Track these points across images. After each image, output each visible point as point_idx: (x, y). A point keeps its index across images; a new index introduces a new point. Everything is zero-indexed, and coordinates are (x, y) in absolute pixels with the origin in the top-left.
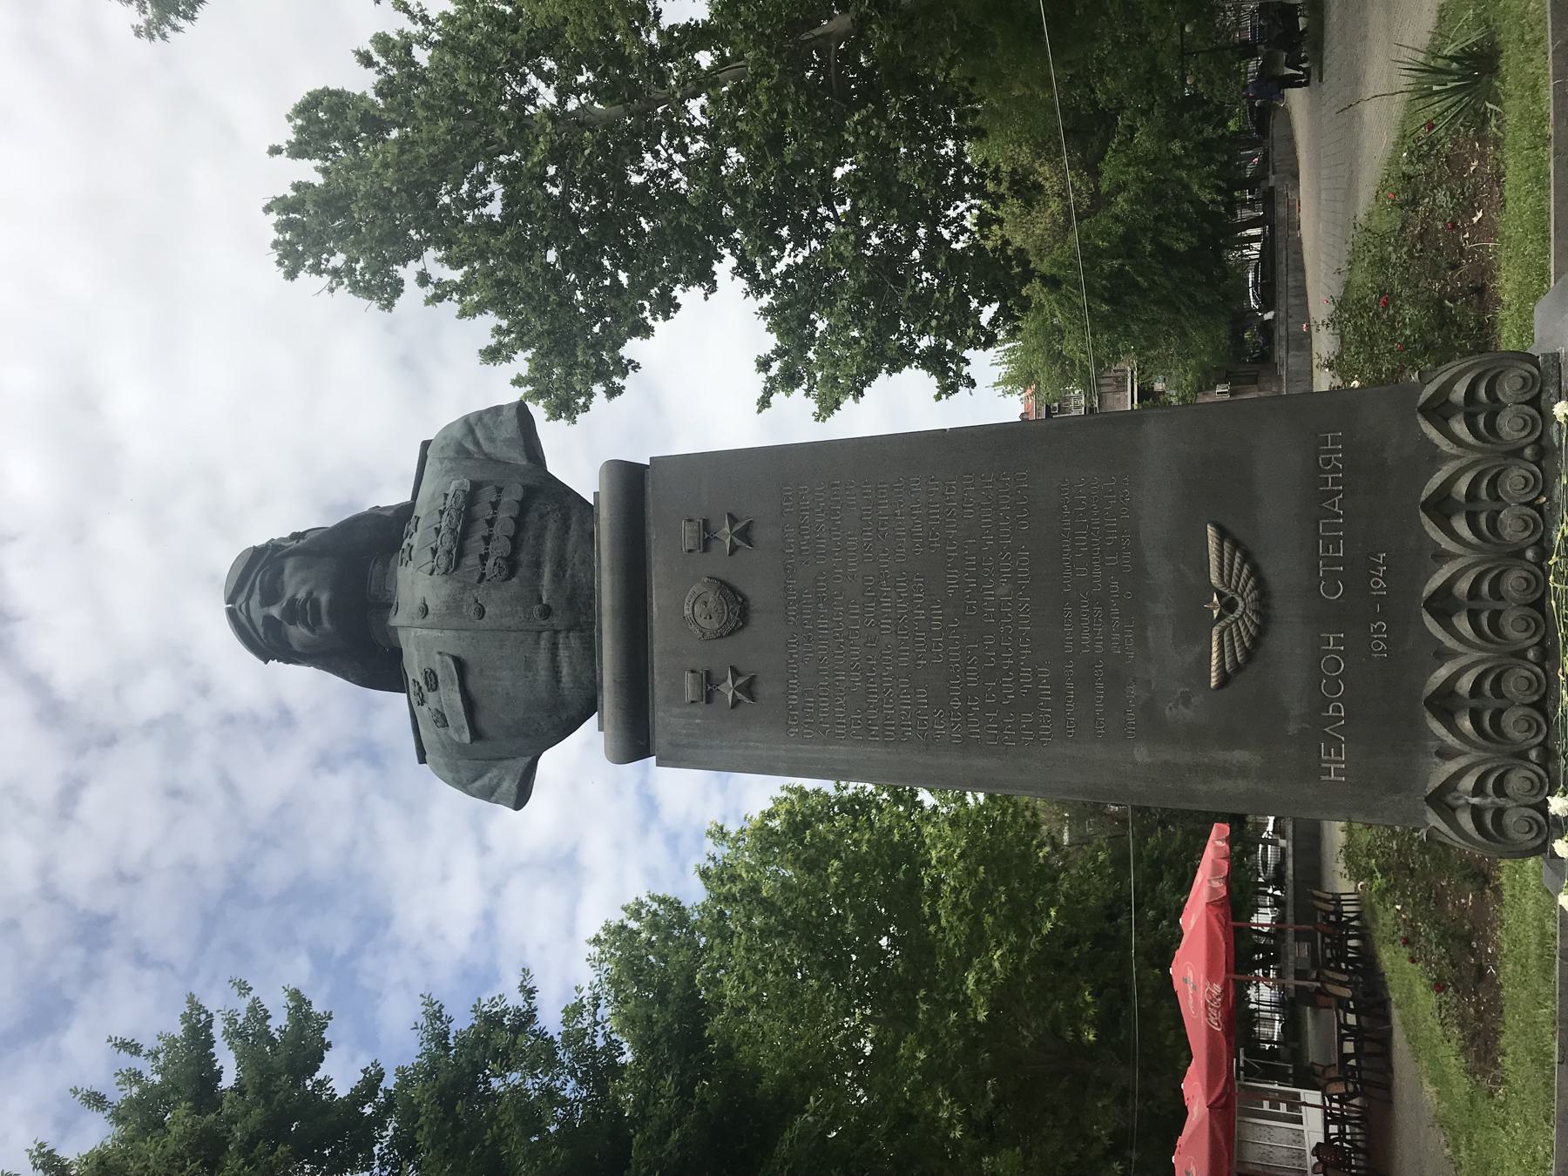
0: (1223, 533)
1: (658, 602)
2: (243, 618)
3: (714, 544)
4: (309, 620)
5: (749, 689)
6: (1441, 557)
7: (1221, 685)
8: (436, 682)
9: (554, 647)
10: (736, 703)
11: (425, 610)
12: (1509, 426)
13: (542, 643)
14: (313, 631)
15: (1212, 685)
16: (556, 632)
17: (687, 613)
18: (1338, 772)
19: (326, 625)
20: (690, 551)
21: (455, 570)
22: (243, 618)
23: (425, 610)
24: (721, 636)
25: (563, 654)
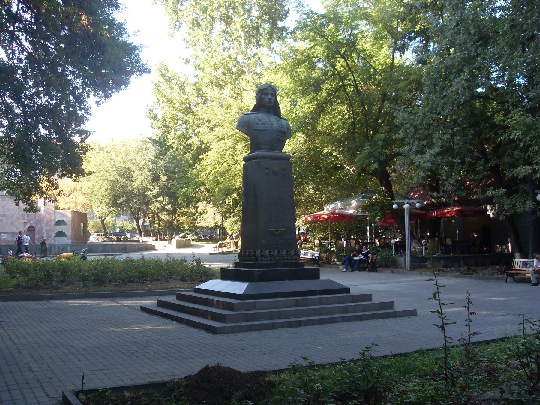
1: (275, 162)
2: (269, 89)
5: (267, 174)
6: (283, 251)
11: (272, 124)
12: (294, 257)
19: (268, 104)
22: (269, 89)
23: (272, 124)
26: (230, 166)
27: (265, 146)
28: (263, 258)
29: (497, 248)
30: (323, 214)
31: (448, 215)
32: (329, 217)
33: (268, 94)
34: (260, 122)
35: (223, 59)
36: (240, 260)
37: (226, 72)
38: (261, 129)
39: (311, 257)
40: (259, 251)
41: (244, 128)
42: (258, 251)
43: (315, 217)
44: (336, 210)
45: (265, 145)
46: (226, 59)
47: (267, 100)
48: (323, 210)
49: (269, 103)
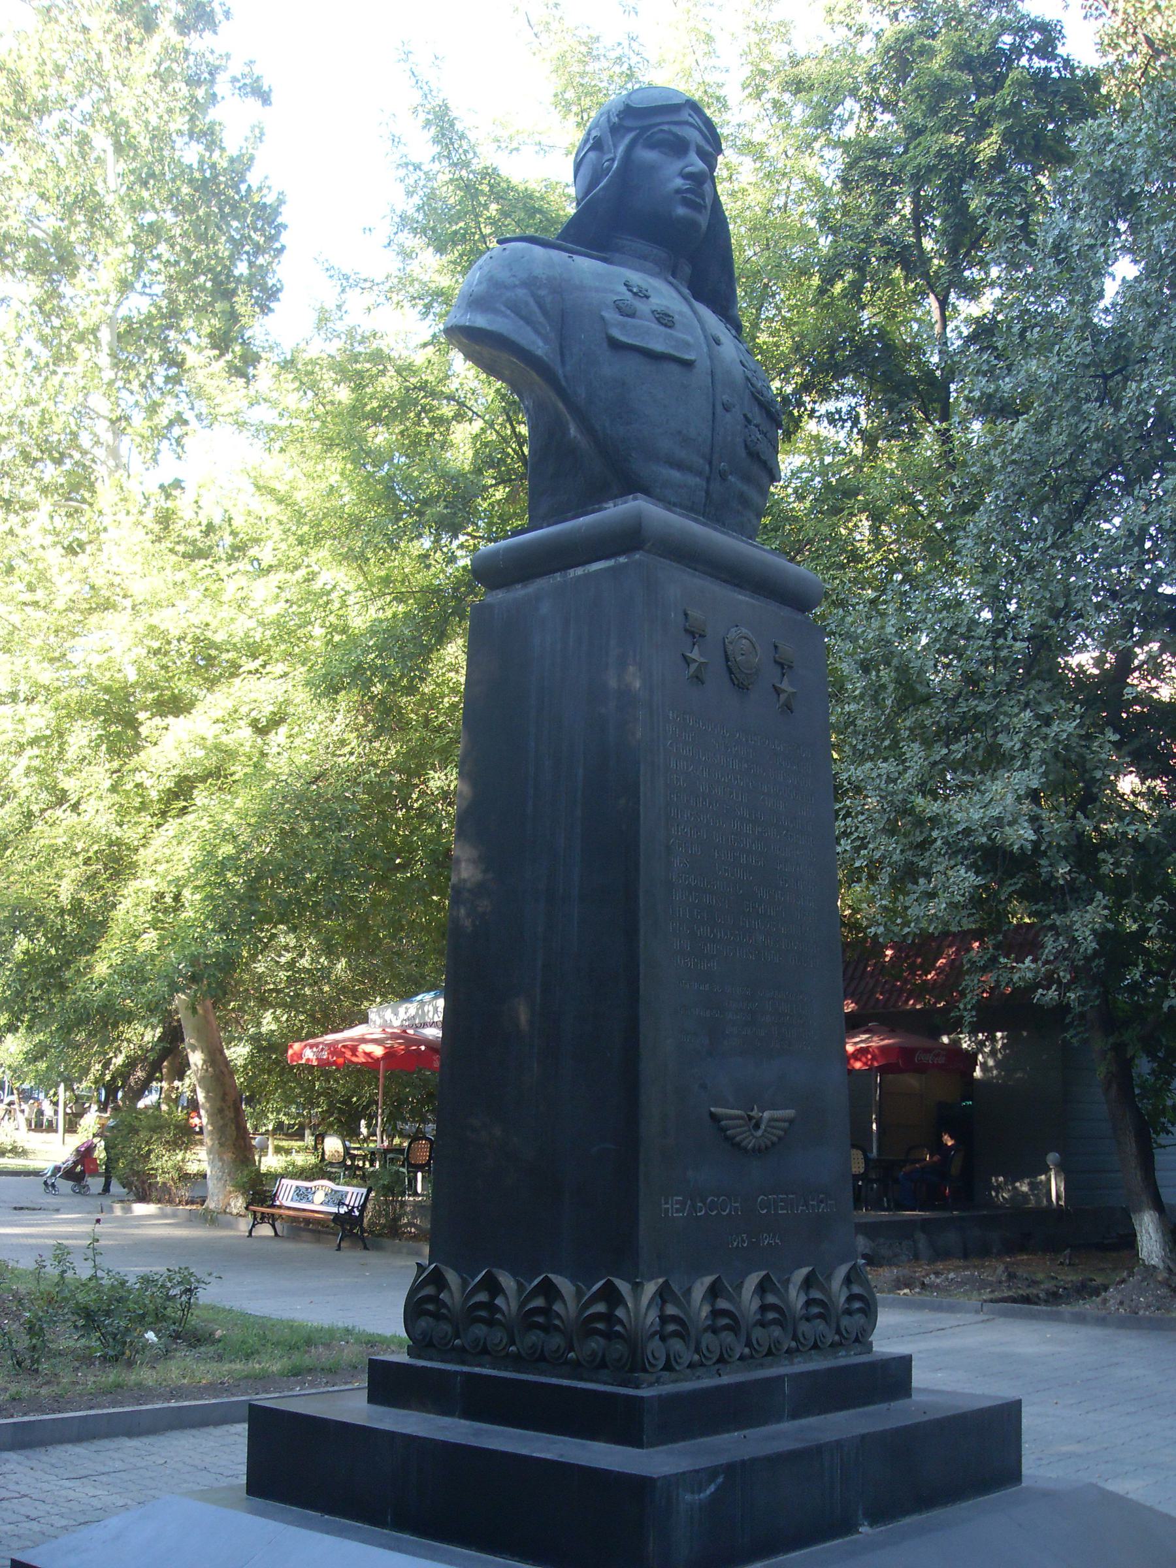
0: (791, 1121)
3: (778, 670)
4: (689, 196)
5: (698, 679)
7: (713, 1116)
8: (666, 326)
9: (699, 474)
10: (687, 661)
13: (701, 461)
14: (678, 191)
15: (712, 1109)
16: (708, 480)
17: (744, 630)
18: (667, 1210)
19: (681, 211)
20: (776, 647)
21: (752, 393)
24: (727, 660)
25: (693, 480)
26: (30, 815)
27: (676, 475)
28: (677, 1345)
29: (998, 1189)
30: (364, 1040)
31: (858, 1065)
32: (390, 1054)
33: (679, 147)
34: (642, 306)
35: (30, 402)
36: (420, 1343)
37: (36, 454)
38: (658, 347)
39: (334, 1210)
40: (650, 1288)
41: (528, 321)
42: (637, 1287)
43: (333, 1048)
44: (424, 1025)
45: (679, 466)
46: (42, 405)
47: (679, 182)
48: (365, 1020)
49: (687, 203)
